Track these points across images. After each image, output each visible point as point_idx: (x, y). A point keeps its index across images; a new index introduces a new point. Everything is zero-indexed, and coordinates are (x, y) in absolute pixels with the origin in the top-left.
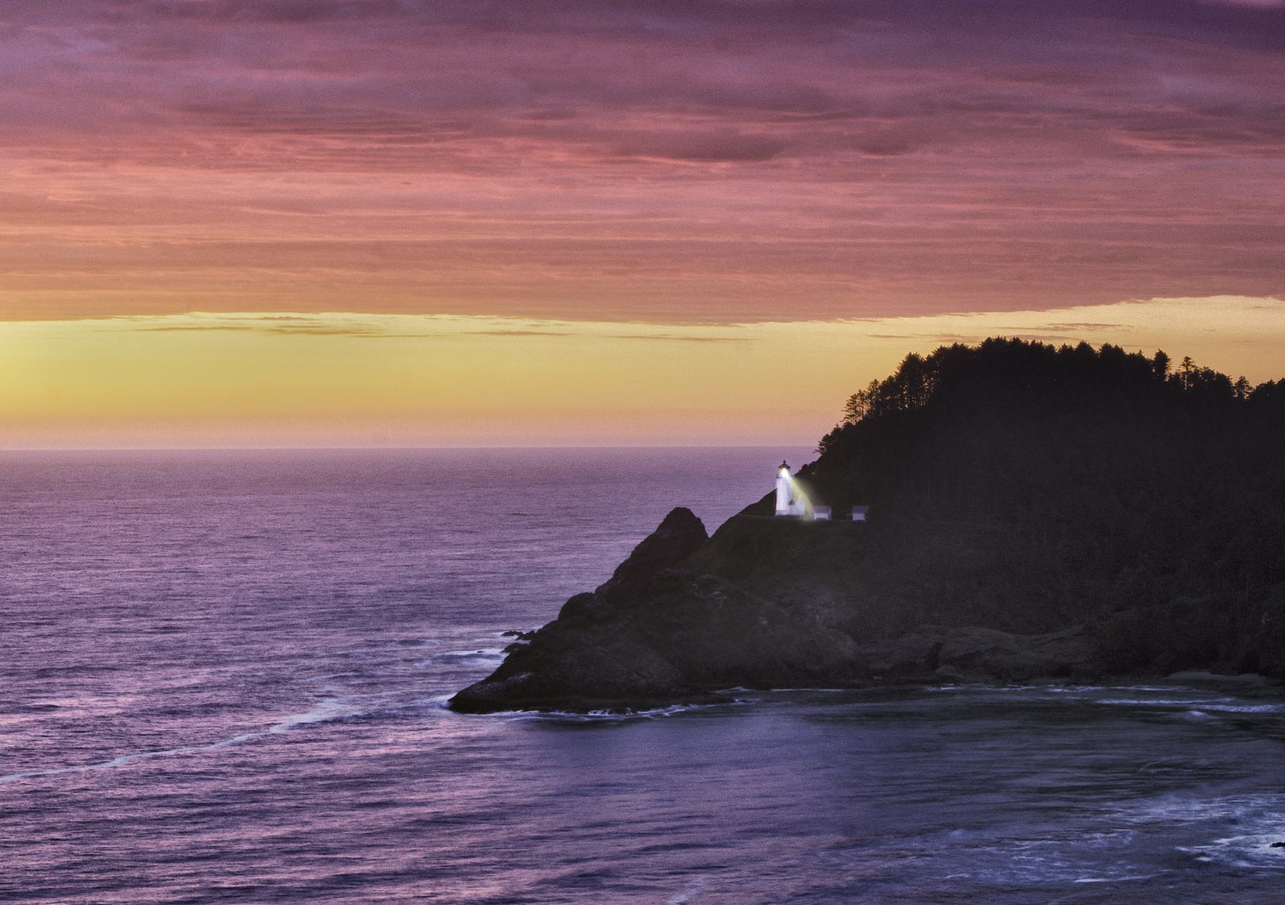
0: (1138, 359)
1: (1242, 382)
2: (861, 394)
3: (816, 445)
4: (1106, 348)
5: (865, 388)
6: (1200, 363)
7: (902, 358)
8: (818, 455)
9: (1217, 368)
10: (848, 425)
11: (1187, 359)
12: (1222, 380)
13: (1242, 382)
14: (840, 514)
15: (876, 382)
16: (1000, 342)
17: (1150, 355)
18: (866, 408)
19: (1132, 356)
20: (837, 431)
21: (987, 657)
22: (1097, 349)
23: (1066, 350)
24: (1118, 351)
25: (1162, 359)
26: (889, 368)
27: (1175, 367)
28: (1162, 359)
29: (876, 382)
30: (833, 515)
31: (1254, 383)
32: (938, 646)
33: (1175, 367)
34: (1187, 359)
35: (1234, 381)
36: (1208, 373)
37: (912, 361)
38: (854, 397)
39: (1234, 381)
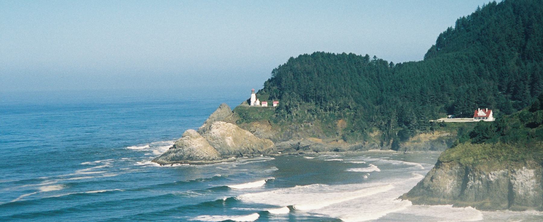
0: (360, 57)
4: (351, 54)
6: (379, 57)
7: (289, 58)
10: (272, 78)
12: (385, 63)
13: (392, 63)
19: (358, 56)
24: (354, 55)
25: (367, 57)
26: (285, 61)
27: (371, 58)
28: (367, 57)
31: (395, 63)
33: (371, 58)
38: (274, 70)
39: (389, 63)
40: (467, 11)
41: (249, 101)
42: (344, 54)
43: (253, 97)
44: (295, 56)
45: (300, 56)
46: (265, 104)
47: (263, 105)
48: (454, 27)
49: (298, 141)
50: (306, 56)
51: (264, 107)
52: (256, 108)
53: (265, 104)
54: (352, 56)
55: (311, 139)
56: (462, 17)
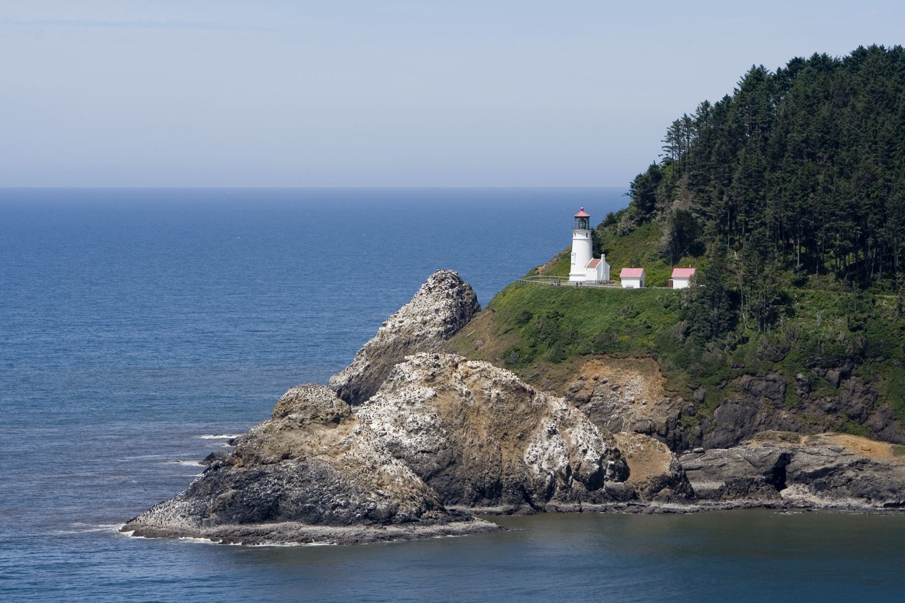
2: (687, 120)
3: (627, 187)
5: (692, 110)
7: (741, 71)
10: (668, 162)
15: (706, 104)
20: (653, 169)
21: (850, 474)
26: (723, 85)
29: (706, 104)
30: (646, 283)
32: (785, 459)
37: (756, 77)
38: (677, 124)
41: (565, 260)
43: (580, 246)
44: (775, 63)
45: (796, 63)
46: (631, 279)
47: (625, 284)
49: (784, 447)
50: (821, 63)
51: (631, 292)
52: (592, 294)
53: (631, 279)
55: (843, 440)
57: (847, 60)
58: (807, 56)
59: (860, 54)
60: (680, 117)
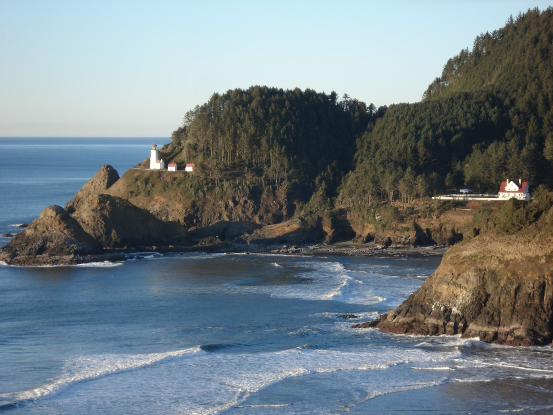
0: (323, 95)
1: (372, 106)
4: (308, 91)
5: (193, 108)
6: (353, 96)
8: (171, 141)
9: (360, 100)
10: (185, 127)
11: (346, 95)
12: (363, 104)
13: (372, 106)
14: (181, 167)
15: (198, 106)
16: (258, 88)
17: (328, 93)
18: (193, 118)
19: (320, 94)
22: (303, 90)
23: (289, 92)
25: (334, 95)
26: (204, 99)
28: (334, 95)
29: (198, 106)
31: (377, 106)
33: (340, 99)
34: (346, 95)
35: (368, 105)
36: (355, 102)
37: (216, 97)
38: (188, 113)
39: (368, 105)
40: (495, 23)
42: (298, 90)
44: (222, 91)
45: (230, 92)
48: (471, 50)
50: (239, 92)
51: (171, 173)
54: (310, 94)
56: (484, 33)
57: (247, 91)
58: (233, 89)
59: (252, 89)
60: (189, 110)
